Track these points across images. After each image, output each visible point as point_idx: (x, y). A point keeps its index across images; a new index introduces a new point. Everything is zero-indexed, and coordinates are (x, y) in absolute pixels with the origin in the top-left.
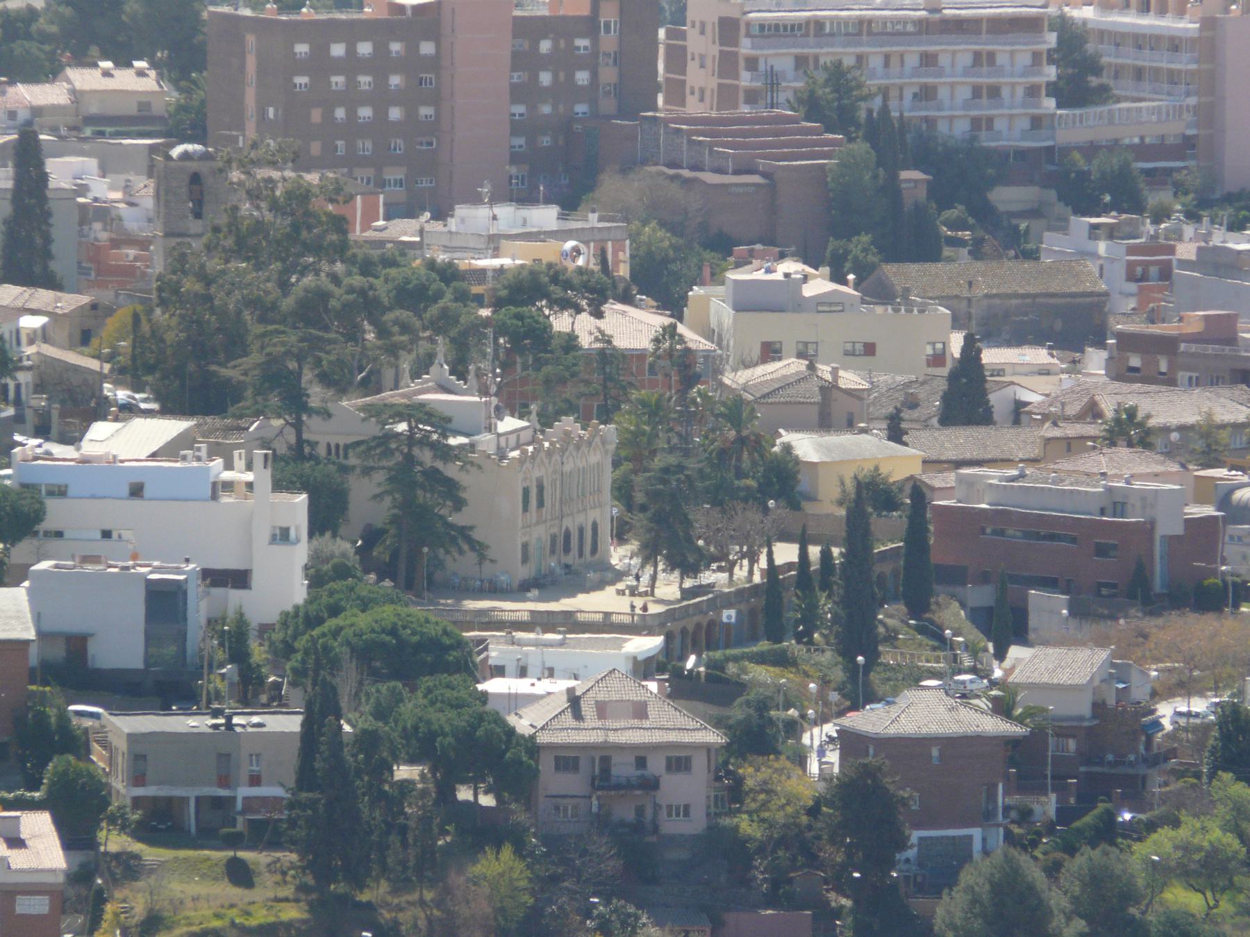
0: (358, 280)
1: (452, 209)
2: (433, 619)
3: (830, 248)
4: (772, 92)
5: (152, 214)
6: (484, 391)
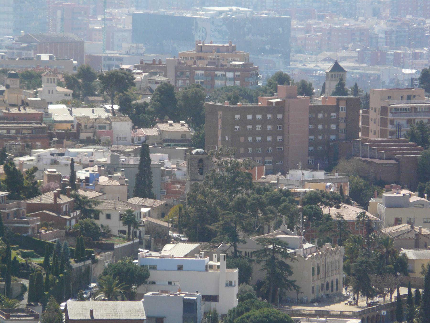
0: (256, 196)
1: (288, 171)
2: (281, 313)
3: (419, 185)
4: (399, 131)
5: (186, 173)
6: (299, 234)
